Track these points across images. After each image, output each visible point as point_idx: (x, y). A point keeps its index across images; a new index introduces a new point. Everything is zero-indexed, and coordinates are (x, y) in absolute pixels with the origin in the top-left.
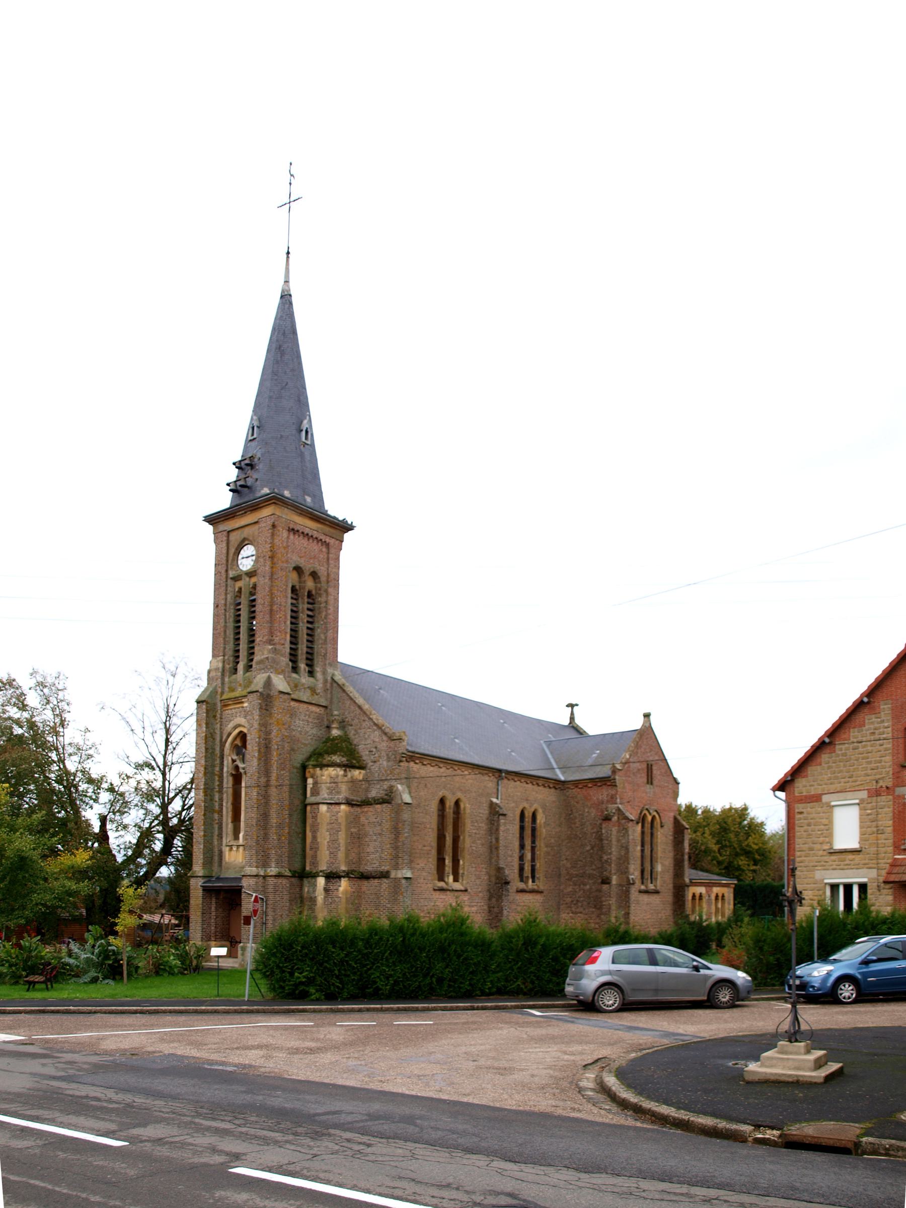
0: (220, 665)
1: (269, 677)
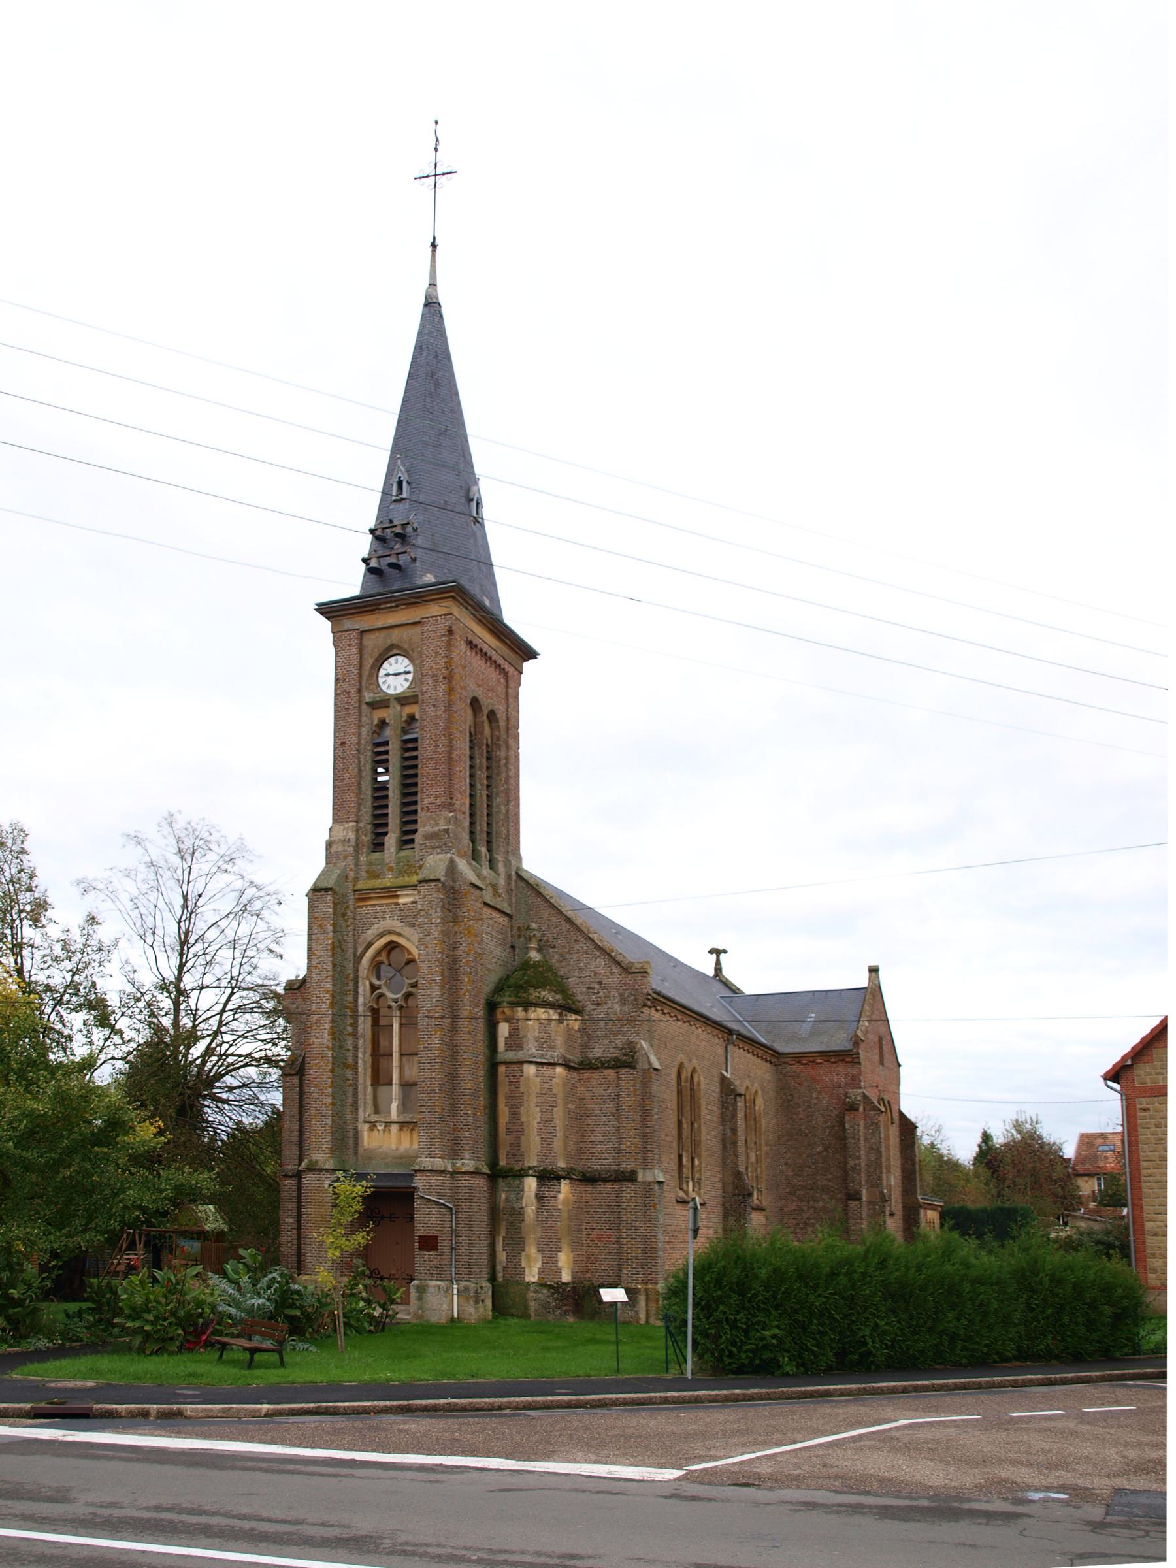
0: (352, 835)
1: (452, 861)
